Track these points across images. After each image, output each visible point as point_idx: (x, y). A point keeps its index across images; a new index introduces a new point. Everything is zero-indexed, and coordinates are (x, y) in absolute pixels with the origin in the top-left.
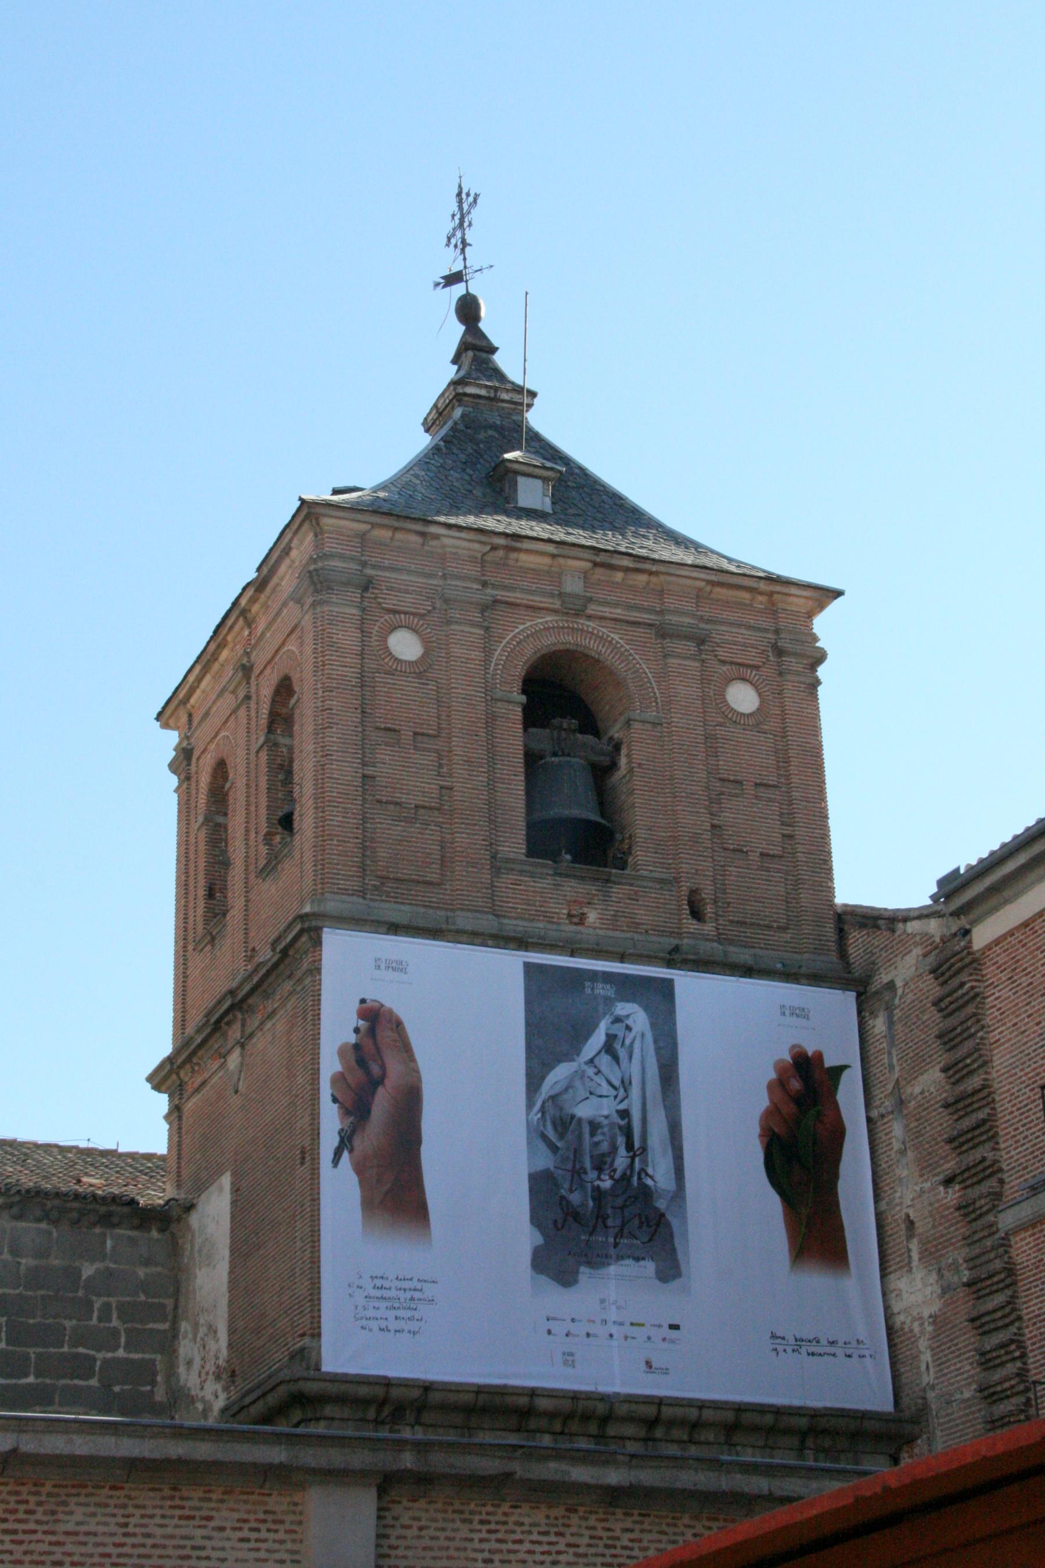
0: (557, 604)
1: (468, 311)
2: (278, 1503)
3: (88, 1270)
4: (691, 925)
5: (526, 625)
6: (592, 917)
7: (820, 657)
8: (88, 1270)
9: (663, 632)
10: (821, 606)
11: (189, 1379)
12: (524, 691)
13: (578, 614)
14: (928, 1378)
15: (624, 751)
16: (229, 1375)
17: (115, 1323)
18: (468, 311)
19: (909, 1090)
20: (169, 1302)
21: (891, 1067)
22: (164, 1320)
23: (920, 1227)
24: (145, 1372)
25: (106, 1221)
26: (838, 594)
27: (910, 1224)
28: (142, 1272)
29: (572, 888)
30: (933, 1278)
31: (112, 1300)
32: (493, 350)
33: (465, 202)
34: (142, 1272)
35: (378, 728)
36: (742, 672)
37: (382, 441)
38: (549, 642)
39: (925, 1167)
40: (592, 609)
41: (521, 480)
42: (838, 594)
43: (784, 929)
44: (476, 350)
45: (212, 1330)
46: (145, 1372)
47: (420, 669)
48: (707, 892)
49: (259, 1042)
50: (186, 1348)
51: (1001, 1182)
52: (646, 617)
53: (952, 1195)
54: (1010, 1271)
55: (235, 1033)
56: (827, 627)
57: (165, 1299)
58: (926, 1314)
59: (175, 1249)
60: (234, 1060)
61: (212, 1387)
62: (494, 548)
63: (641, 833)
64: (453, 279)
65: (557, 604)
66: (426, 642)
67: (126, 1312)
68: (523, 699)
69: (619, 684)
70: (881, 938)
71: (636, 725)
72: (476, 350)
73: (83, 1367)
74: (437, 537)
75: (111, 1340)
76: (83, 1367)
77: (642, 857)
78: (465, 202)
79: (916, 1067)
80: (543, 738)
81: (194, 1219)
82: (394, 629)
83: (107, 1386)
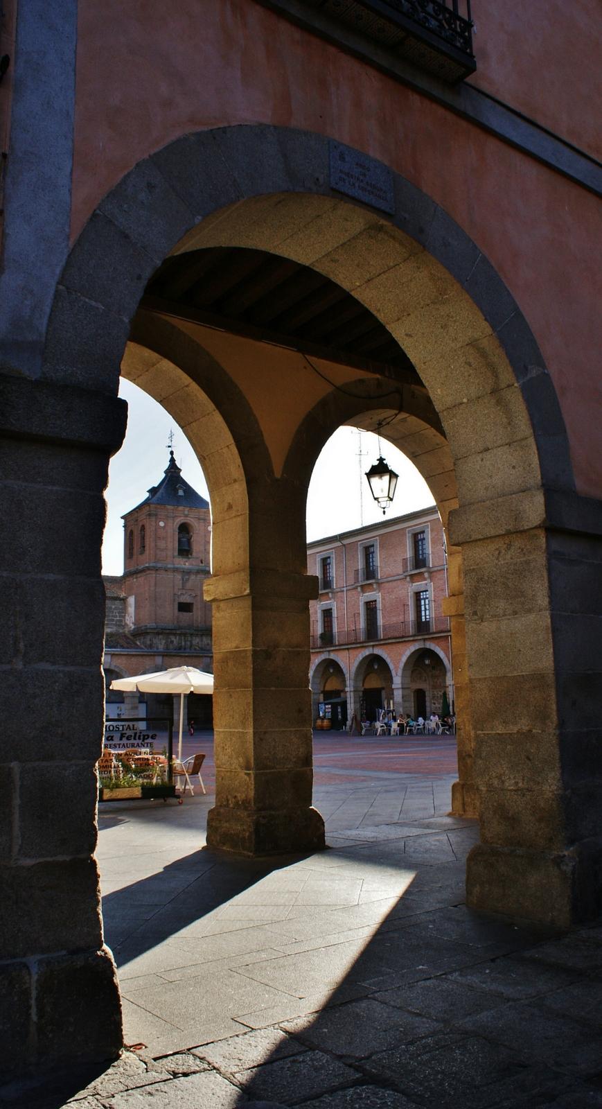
1: (172, 453)
2: (152, 657)
3: (113, 607)
4: (201, 564)
5: (179, 519)
6: (187, 564)
8: (113, 607)
11: (128, 622)
16: (135, 624)
18: (172, 453)
24: (121, 621)
28: (121, 607)
29: (185, 560)
34: (121, 607)
37: (157, 478)
38: (182, 521)
44: (172, 460)
45: (131, 617)
46: (121, 621)
47: (164, 527)
49: (140, 579)
50: (127, 618)
55: (135, 576)
57: (124, 611)
59: (125, 603)
60: (135, 580)
61: (131, 625)
63: (194, 551)
64: (169, 447)
66: (165, 523)
69: (192, 527)
72: (172, 460)
73: (113, 620)
75: (116, 617)
76: (113, 620)
77: (194, 554)
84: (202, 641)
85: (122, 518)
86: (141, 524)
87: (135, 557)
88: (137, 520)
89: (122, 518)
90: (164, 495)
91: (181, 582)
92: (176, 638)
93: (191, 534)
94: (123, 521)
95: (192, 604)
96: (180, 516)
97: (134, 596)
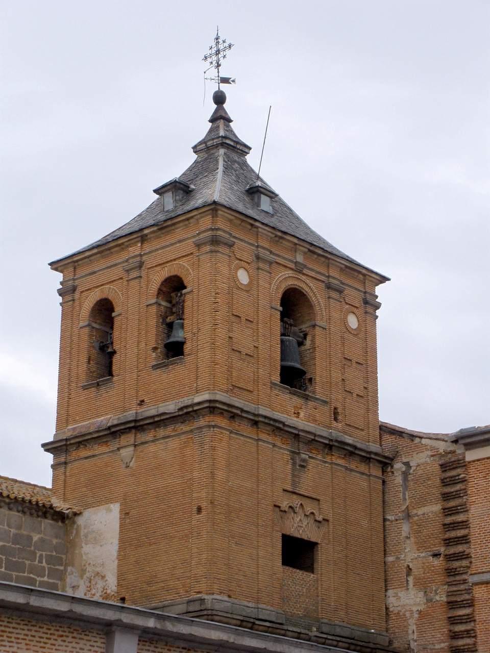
0: (292, 266)
1: (219, 99)
3: (36, 537)
7: (377, 306)
8: (36, 537)
9: (329, 287)
10: (381, 282)
12: (282, 305)
13: (301, 272)
15: (309, 338)
17: (44, 564)
18: (219, 99)
19: (415, 511)
20: (64, 556)
21: (405, 499)
22: (61, 565)
23: (415, 571)
25: (45, 515)
26: (388, 279)
27: (409, 570)
30: (421, 594)
31: (44, 553)
32: (230, 121)
34: (55, 541)
35: (233, 315)
40: (305, 271)
41: (263, 197)
42: (388, 279)
43: (362, 430)
44: (220, 118)
47: (248, 289)
48: (339, 410)
51: (471, 562)
52: (323, 278)
53: (438, 563)
56: (380, 290)
58: (415, 609)
62: (276, 236)
65: (292, 266)
67: (50, 560)
68: (281, 309)
70: (405, 442)
71: (317, 328)
72: (220, 118)
74: (257, 227)
79: (422, 501)
81: (80, 521)
85: (56, 265)
86: (157, 278)
88: (141, 266)
89: (56, 265)
94: (58, 277)
95: (316, 544)
97: (116, 508)
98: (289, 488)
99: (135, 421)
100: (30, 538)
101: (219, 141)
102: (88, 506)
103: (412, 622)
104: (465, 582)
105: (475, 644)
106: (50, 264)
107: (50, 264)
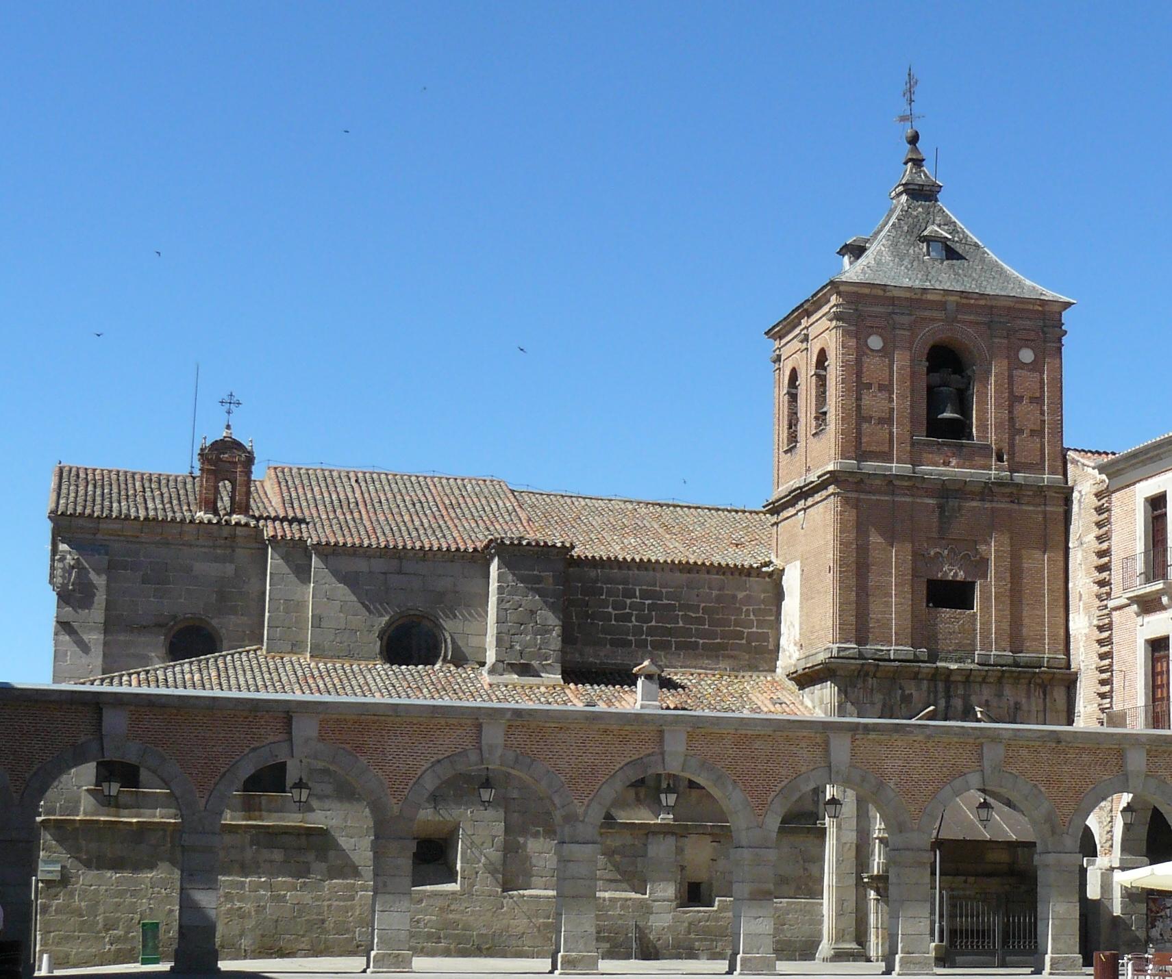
3: (740, 595)
8: (740, 595)
14: (1082, 658)
17: (752, 617)
25: (749, 575)
33: (911, 83)
36: (1027, 343)
39: (1088, 573)
54: (1111, 623)
56: (1066, 316)
64: (903, 119)
78: (911, 83)
79: (1088, 532)
80: (936, 378)
82: (870, 335)
83: (749, 643)
84: (1000, 695)
87: (801, 445)
90: (887, 258)
91: (935, 518)
92: (919, 688)
93: (969, 372)
96: (933, 320)
97: (798, 563)
98: (935, 535)
99: (801, 488)
100: (734, 597)
101: (901, 188)
102: (787, 562)
103: (1081, 644)
104: (1106, 607)
105: (1111, 665)
106: (766, 333)
107: (766, 333)
